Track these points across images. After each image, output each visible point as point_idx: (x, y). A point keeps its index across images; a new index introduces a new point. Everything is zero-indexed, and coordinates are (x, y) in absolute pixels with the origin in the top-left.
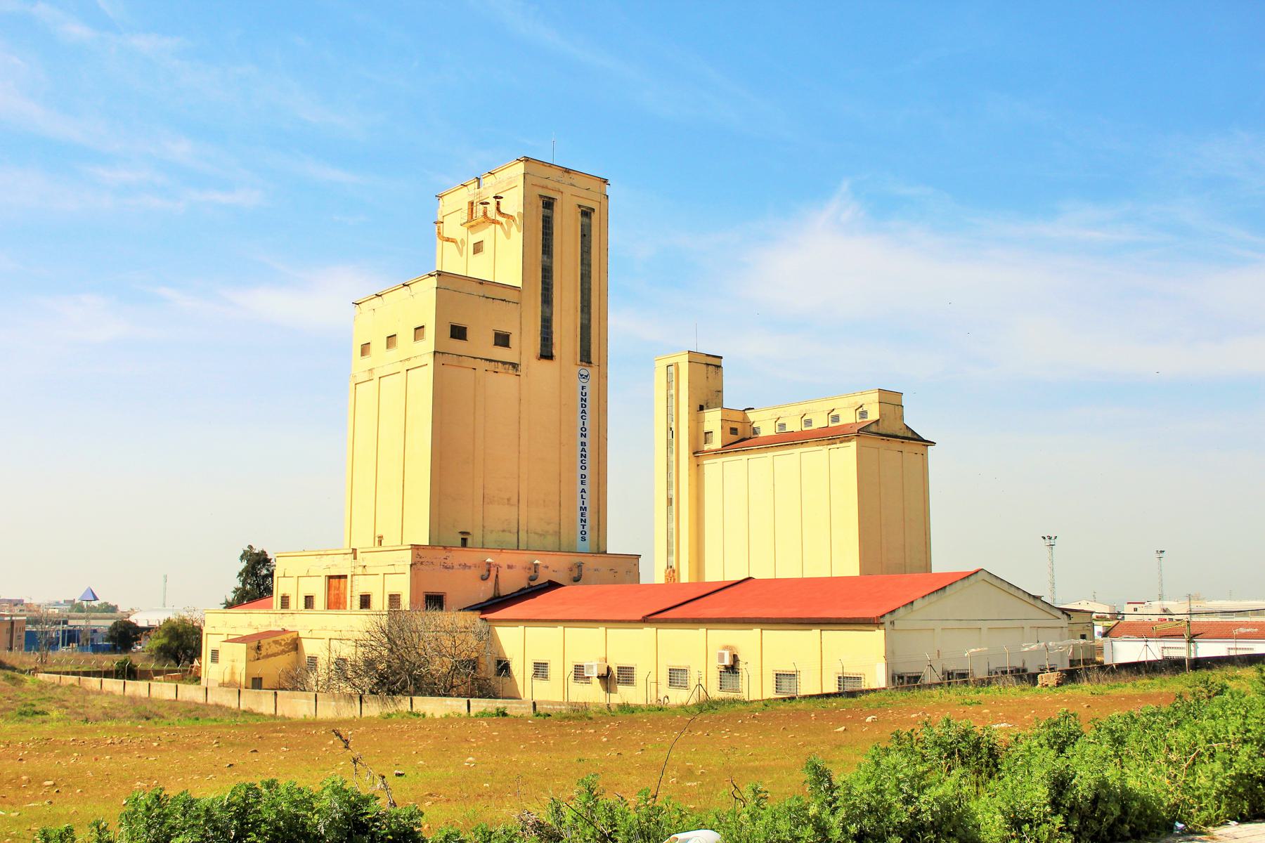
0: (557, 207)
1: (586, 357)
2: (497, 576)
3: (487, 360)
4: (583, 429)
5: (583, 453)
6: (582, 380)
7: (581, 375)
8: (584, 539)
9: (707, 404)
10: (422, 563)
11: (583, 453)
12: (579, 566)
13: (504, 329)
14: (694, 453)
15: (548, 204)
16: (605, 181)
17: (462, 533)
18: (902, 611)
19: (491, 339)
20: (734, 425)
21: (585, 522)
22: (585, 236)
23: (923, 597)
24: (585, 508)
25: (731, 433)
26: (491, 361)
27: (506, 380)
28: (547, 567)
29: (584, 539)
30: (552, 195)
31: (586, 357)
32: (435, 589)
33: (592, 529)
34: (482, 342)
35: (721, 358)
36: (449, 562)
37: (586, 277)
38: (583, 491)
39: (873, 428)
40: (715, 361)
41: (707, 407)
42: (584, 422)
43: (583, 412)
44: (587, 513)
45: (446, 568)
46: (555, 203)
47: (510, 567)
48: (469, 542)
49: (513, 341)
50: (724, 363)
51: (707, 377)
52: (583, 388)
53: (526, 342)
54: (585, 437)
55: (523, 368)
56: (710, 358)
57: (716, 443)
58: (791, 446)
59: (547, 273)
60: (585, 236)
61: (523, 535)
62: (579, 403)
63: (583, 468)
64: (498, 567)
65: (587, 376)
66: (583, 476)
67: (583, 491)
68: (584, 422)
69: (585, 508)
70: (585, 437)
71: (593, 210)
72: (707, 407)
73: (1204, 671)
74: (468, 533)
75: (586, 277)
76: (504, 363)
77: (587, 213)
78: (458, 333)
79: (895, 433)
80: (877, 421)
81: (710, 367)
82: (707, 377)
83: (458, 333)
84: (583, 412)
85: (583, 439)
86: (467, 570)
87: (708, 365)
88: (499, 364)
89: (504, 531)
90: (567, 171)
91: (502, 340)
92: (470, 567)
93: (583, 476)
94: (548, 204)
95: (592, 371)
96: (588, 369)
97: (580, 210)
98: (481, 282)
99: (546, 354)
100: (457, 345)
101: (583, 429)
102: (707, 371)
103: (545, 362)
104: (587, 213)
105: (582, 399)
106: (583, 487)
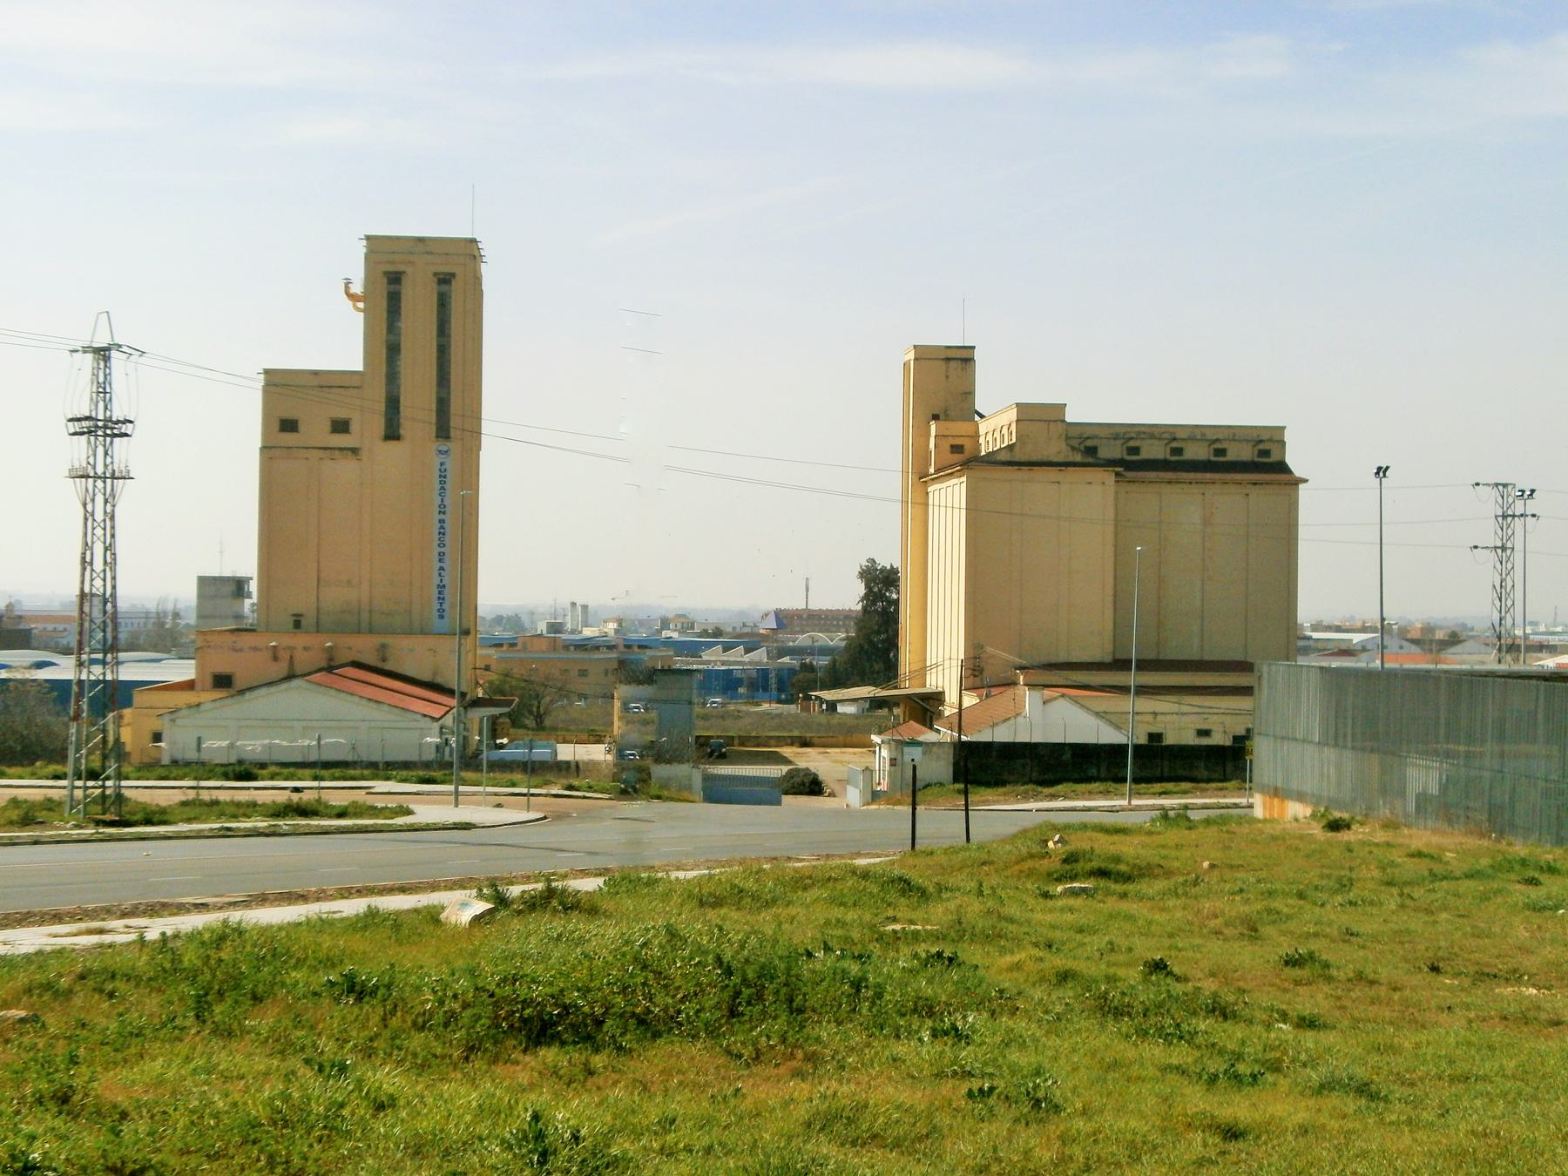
0: (406, 281)
1: (443, 432)
2: (291, 657)
3: (320, 448)
4: (442, 505)
5: (442, 531)
6: (443, 456)
7: (440, 451)
8: (442, 617)
9: (946, 411)
10: (209, 647)
11: (442, 531)
12: (383, 646)
13: (341, 414)
14: (920, 478)
15: (395, 278)
16: (473, 241)
17: (294, 615)
18: (184, 712)
19: (327, 426)
20: (958, 442)
21: (443, 599)
22: (443, 303)
23: (213, 701)
24: (444, 586)
25: (952, 452)
26: (325, 449)
27: (346, 469)
28: (350, 648)
29: (442, 617)
30: (401, 268)
31: (443, 432)
32: (224, 669)
33: (453, 606)
34: (315, 430)
35: (973, 348)
36: (238, 646)
37: (443, 352)
38: (442, 569)
39: (1003, 457)
40: (964, 354)
41: (947, 415)
42: (442, 500)
43: (443, 488)
44: (446, 591)
45: (236, 651)
46: (403, 277)
47: (305, 649)
48: (304, 622)
49: (354, 427)
50: (977, 355)
51: (947, 377)
52: (442, 464)
53: (366, 425)
54: (444, 513)
55: (364, 454)
56: (949, 350)
57: (932, 470)
58: (946, 478)
59: (393, 350)
60: (443, 303)
61: (365, 616)
62: (438, 480)
63: (441, 545)
64: (292, 648)
65: (446, 452)
66: (442, 554)
67: (442, 569)
68: (442, 500)
69: (444, 586)
70: (444, 513)
71: (453, 275)
72: (947, 415)
73: (1071, 784)
74: (301, 615)
75: (443, 352)
76: (341, 449)
77: (445, 280)
78: (289, 426)
79: (1045, 459)
80: (1010, 447)
81: (953, 364)
82: (947, 377)
83: (289, 426)
84: (443, 488)
85: (442, 516)
86: (258, 653)
87: (948, 359)
88: (337, 452)
89: (343, 612)
90: (421, 240)
91: (341, 426)
92: (260, 650)
93: (442, 554)
94: (395, 278)
95: (454, 446)
96: (448, 444)
97: (435, 280)
98: (316, 373)
99: (392, 434)
100: (289, 439)
101: (442, 505)
102: (948, 368)
103: (392, 444)
104: (445, 280)
105: (440, 476)
106: (442, 564)
